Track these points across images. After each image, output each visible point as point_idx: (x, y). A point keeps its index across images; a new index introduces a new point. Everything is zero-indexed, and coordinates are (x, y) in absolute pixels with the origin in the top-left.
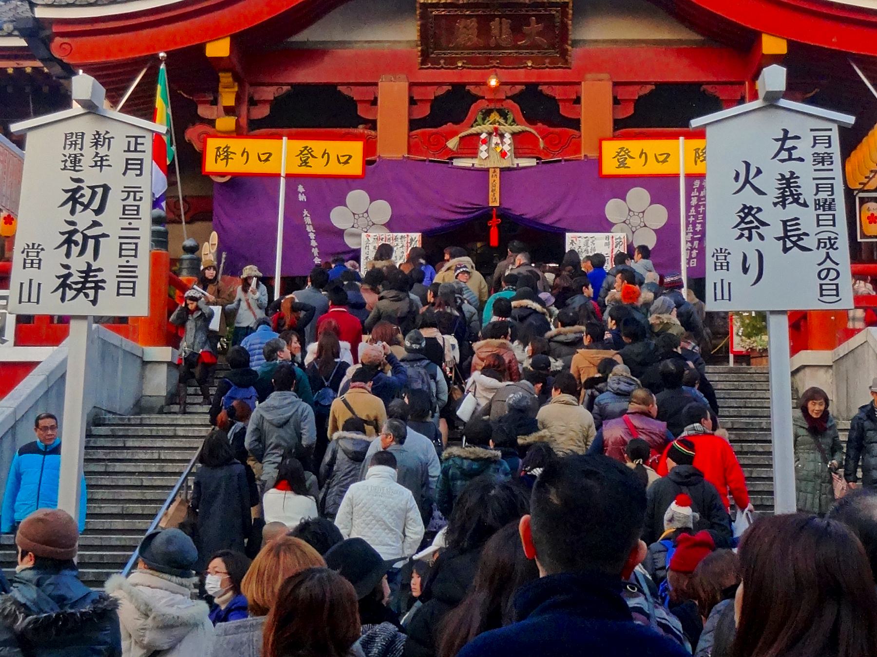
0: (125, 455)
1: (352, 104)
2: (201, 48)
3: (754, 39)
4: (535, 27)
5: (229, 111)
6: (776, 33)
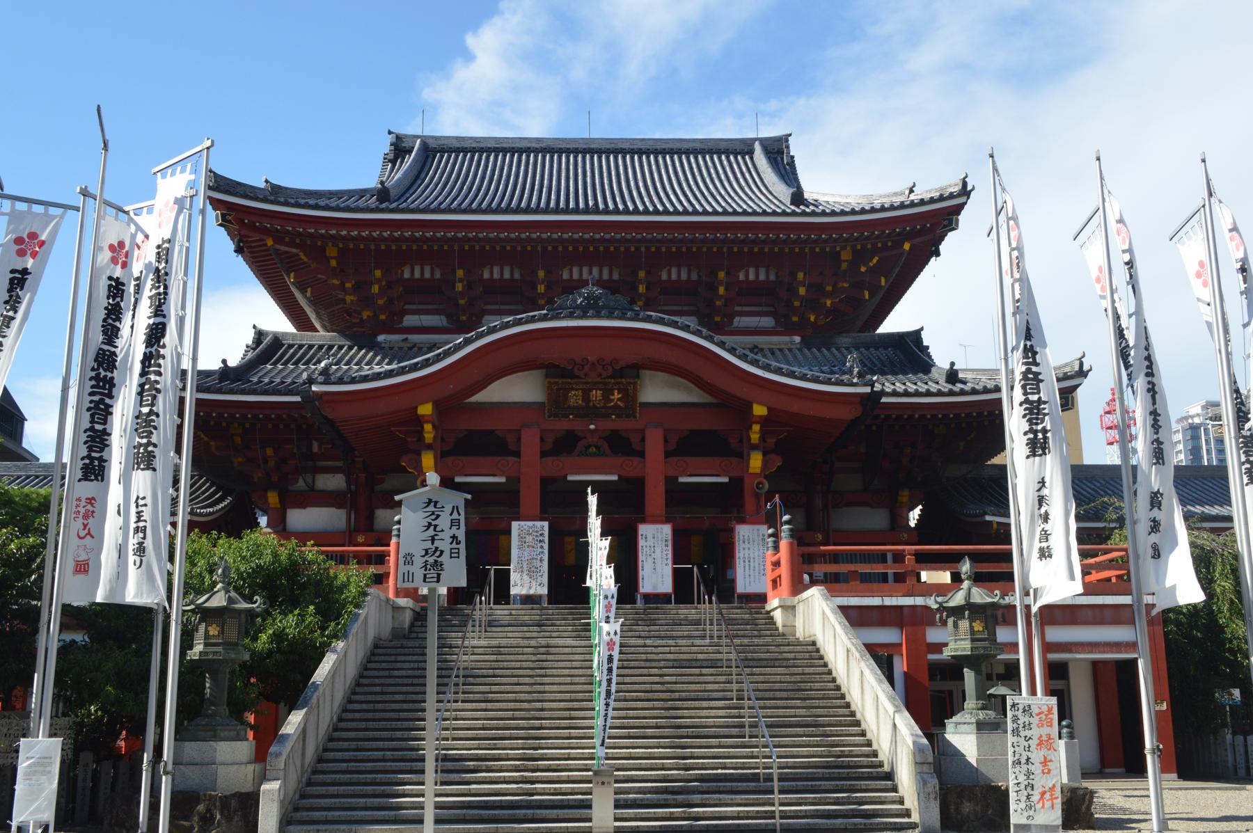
0: (399, 665)
2: (416, 408)
3: (749, 406)
4: (617, 395)
5: (429, 447)
6: (759, 403)
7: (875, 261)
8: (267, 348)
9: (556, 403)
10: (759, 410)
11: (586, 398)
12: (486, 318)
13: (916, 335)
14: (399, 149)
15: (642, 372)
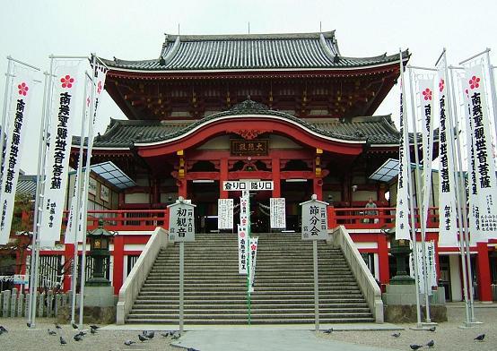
1: (214, 165)
5: (182, 168)
8: (115, 126)
9: (234, 150)
10: (319, 151)
11: (247, 146)
12: (206, 113)
13: (388, 118)
14: (170, 41)
15: (271, 136)
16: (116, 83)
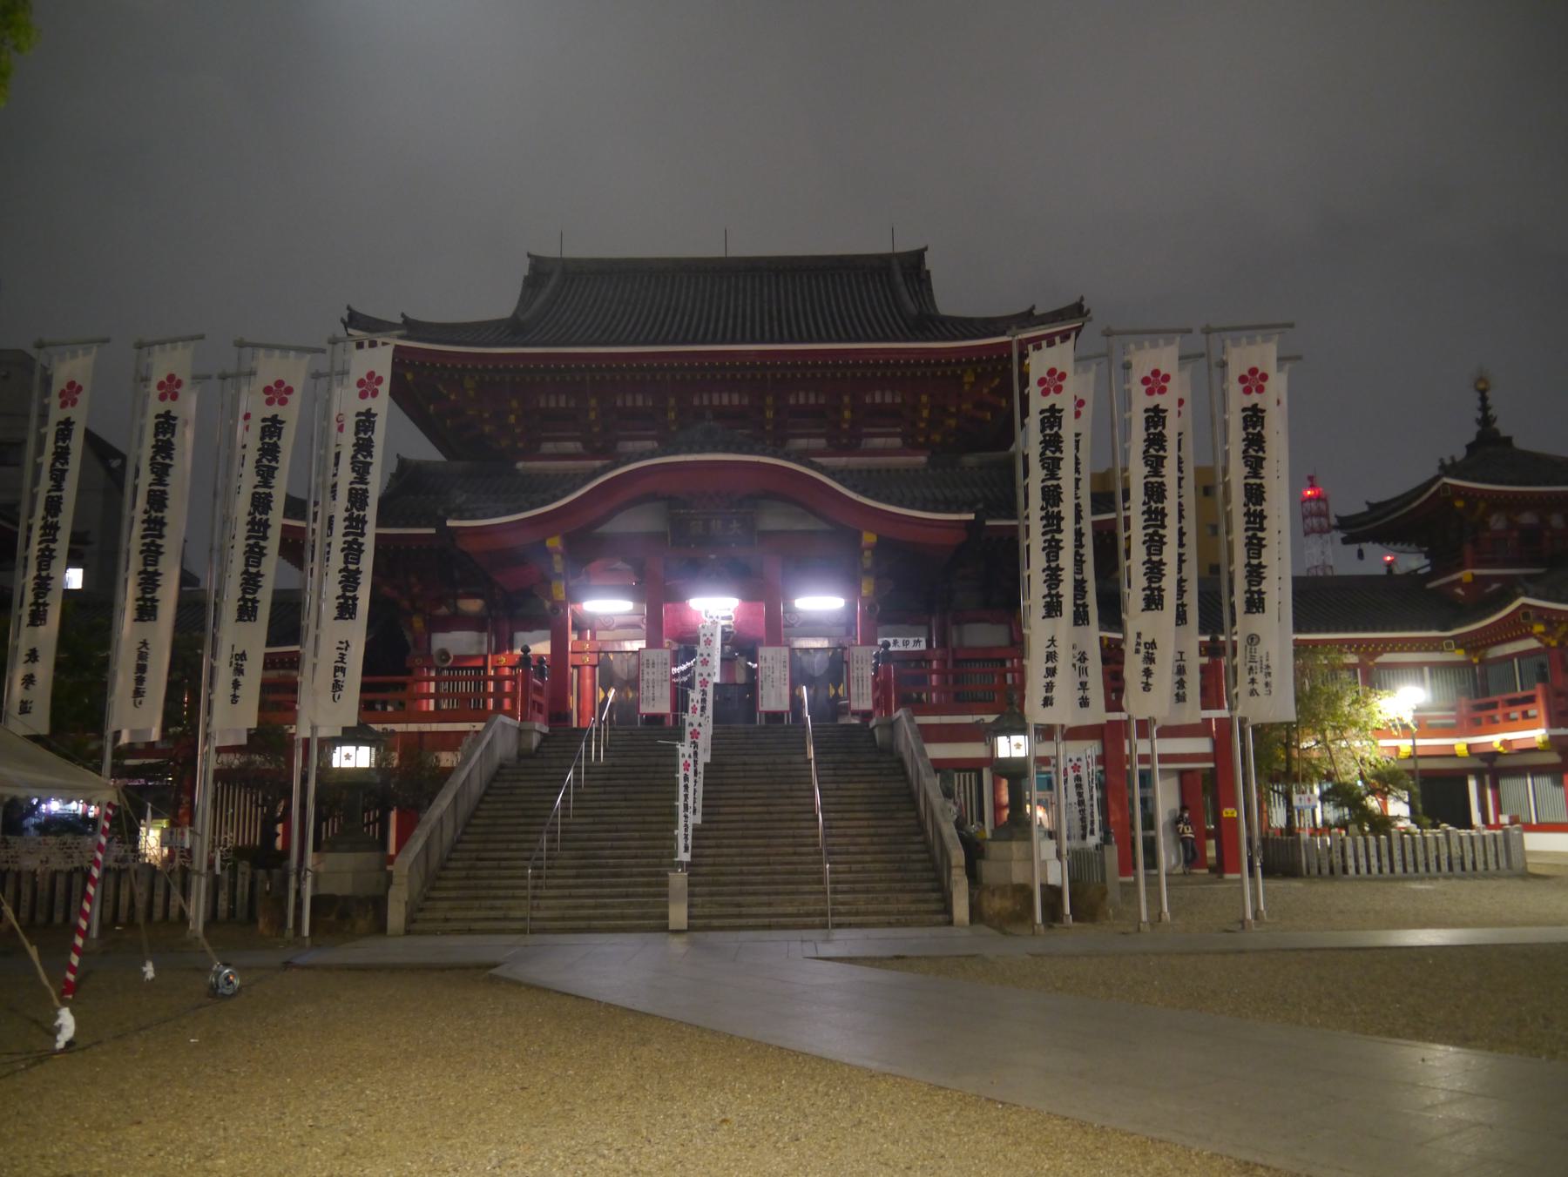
7: (997, 381)
14: (540, 272)
16: (409, 376)
